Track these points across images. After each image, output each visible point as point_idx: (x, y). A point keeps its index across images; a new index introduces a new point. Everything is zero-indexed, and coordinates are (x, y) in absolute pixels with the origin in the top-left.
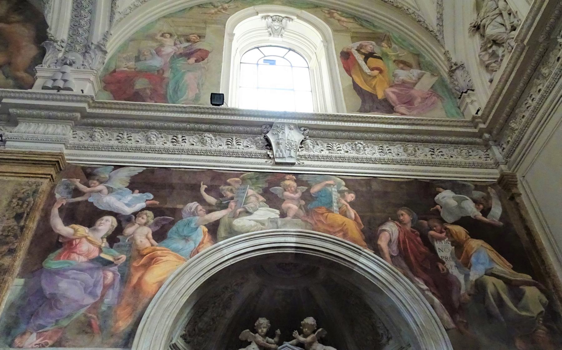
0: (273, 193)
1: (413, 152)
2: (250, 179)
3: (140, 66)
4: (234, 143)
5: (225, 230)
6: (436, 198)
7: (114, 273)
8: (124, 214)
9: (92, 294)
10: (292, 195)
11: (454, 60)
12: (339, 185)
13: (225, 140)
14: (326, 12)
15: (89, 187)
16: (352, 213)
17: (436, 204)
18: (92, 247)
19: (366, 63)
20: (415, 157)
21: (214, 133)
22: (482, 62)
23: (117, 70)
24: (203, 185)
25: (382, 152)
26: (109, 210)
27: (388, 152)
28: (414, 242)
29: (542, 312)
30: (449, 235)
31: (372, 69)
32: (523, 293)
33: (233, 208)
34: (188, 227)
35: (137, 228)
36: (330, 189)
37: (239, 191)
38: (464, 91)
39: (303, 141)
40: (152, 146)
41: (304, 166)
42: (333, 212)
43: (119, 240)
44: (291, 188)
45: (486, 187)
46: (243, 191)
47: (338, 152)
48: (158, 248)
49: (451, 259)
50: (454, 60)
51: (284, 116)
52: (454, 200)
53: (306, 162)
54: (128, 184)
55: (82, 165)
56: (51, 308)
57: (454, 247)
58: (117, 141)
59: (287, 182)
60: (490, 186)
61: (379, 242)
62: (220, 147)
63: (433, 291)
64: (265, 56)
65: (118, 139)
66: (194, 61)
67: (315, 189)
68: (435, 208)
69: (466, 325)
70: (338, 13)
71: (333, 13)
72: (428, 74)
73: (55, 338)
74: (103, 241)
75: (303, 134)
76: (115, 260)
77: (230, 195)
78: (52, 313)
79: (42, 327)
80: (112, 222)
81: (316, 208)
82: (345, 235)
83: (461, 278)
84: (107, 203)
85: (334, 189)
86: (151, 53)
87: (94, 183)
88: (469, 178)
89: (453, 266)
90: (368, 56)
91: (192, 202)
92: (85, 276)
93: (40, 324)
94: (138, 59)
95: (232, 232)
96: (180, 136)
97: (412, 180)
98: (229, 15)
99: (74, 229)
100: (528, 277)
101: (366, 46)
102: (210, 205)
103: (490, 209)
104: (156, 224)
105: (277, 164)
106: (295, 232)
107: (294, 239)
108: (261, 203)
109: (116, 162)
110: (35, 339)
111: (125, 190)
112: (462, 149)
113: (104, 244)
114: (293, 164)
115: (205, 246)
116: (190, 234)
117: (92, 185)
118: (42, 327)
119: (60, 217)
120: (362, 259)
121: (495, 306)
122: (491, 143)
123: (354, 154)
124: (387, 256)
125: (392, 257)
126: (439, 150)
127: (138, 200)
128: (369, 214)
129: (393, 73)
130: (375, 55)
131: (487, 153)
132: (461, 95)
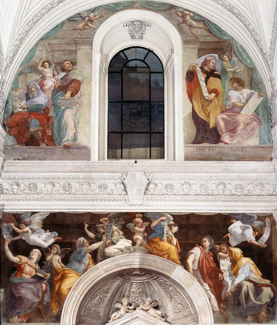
2: (114, 218)
5: (101, 256)
6: (229, 228)
7: (45, 284)
9: (37, 296)
10: (139, 229)
12: (169, 220)
14: (180, 14)
15: (20, 229)
16: (175, 241)
17: (228, 232)
23: (14, 111)
30: (230, 255)
31: (210, 92)
32: (261, 291)
33: (105, 240)
34: (80, 254)
35: (52, 257)
37: (107, 228)
41: (147, 206)
42: (163, 241)
43: (44, 265)
44: (139, 224)
46: (110, 228)
48: (66, 269)
52: (241, 229)
54: (42, 226)
55: (13, 213)
56: (21, 304)
57: (231, 263)
59: (137, 220)
61: (188, 261)
67: (154, 223)
68: (227, 236)
69: (225, 310)
70: (190, 16)
73: (26, 319)
74: (36, 265)
77: (102, 230)
78: (21, 307)
79: (19, 313)
80: (38, 253)
81: (153, 238)
82: (169, 258)
84: (33, 240)
86: (37, 89)
87: (23, 226)
89: (227, 275)
92: (32, 286)
93: (18, 312)
95: (105, 257)
98: (95, 30)
102: (91, 239)
103: (262, 235)
104: (62, 253)
108: (121, 236)
110: (18, 319)
111: (41, 230)
115: (90, 267)
116: (81, 259)
117: (22, 227)
118: (19, 313)
121: (244, 298)
124: (191, 270)
125: (194, 270)
128: (185, 242)
130: (216, 72)
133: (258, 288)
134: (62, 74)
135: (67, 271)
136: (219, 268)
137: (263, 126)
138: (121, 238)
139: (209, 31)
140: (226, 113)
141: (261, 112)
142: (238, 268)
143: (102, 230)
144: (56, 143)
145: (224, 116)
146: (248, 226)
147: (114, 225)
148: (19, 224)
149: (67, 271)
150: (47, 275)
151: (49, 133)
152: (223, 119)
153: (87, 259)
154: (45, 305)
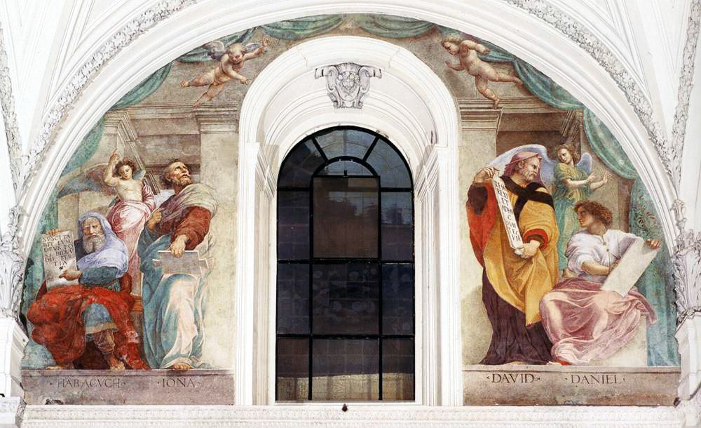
14: (454, 47)
23: (48, 285)
31: (527, 238)
70: (478, 51)
86: (102, 230)
98: (245, 85)
130: (540, 190)
134: (165, 194)
137: (655, 321)
139: (524, 88)
140: (567, 290)
141: (650, 288)
144: (150, 363)
145: (561, 296)
151: (133, 338)
152: (559, 304)
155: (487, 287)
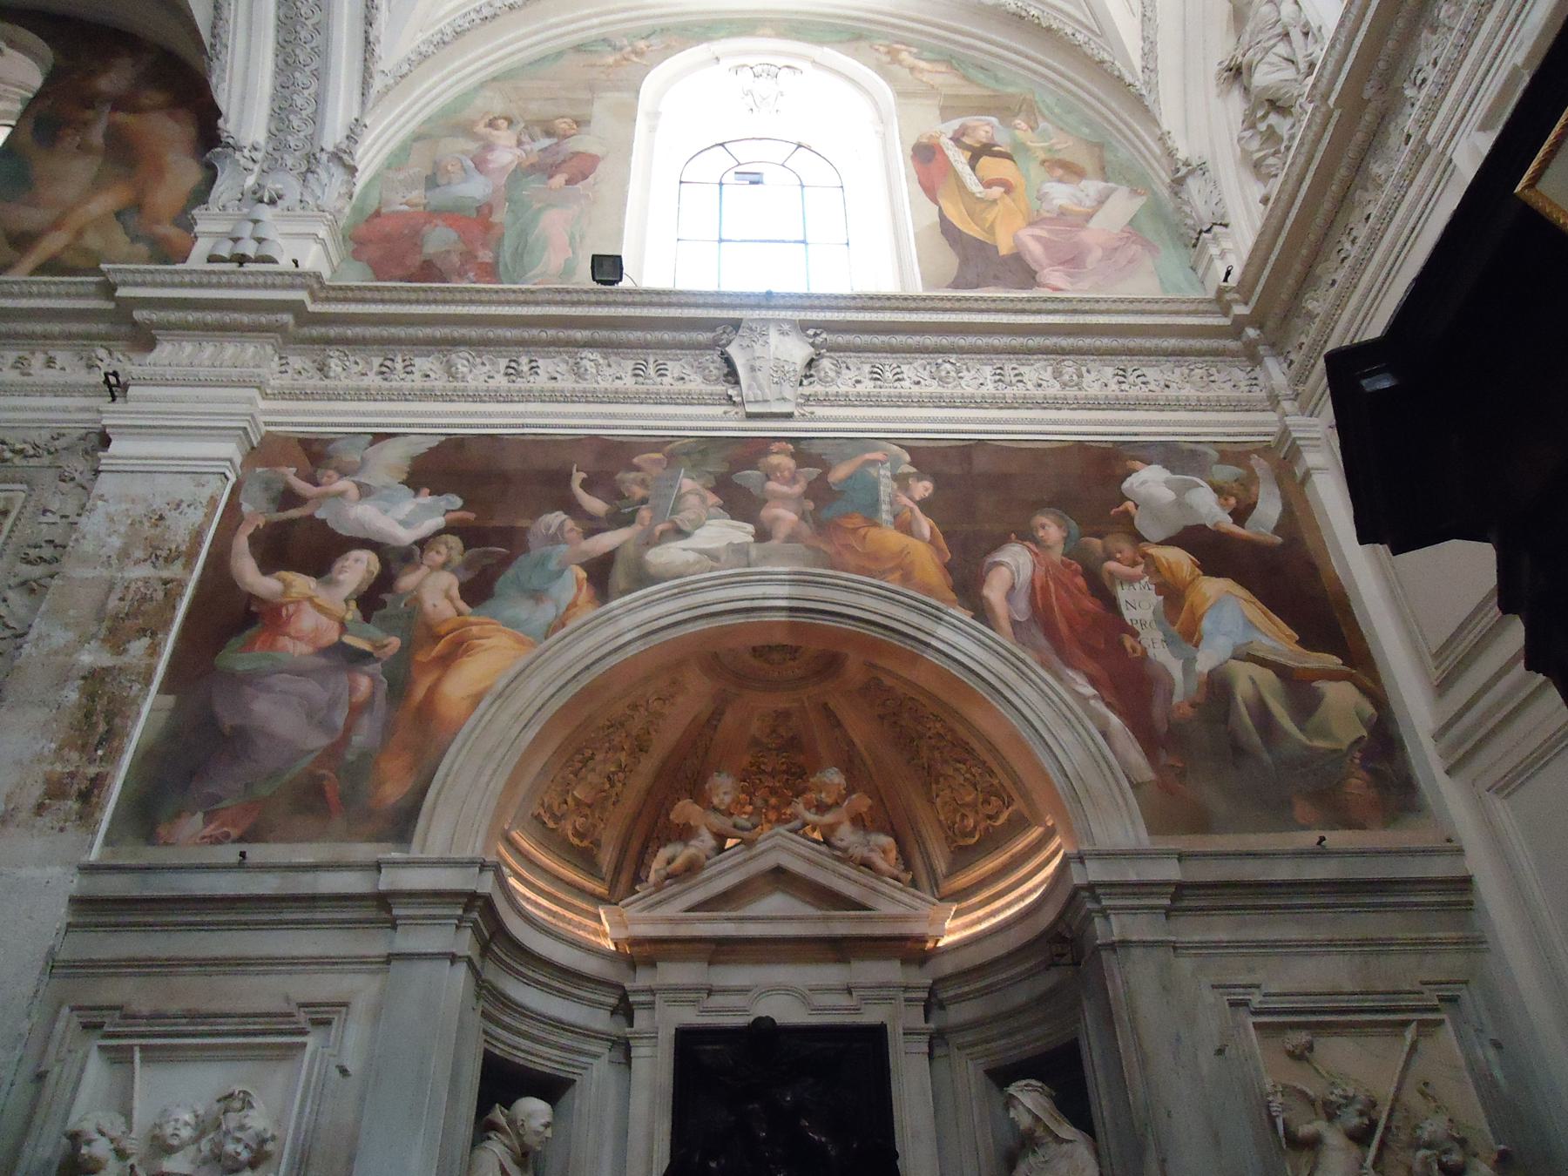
0: (740, 486)
1: (1075, 377)
2: (687, 454)
3: (438, 198)
4: (651, 371)
6: (1126, 485)
7: (372, 677)
8: (395, 544)
9: (324, 725)
10: (785, 489)
11: (1181, 155)
12: (896, 461)
13: (630, 365)
14: (882, 49)
15: (317, 484)
16: (925, 525)
17: (1124, 498)
18: (324, 619)
19: (973, 168)
20: (1080, 389)
21: (605, 350)
22: (1246, 154)
23: (384, 210)
24: (577, 471)
25: (1000, 380)
26: (361, 535)
27: (1014, 380)
28: (1067, 590)
29: (1362, 738)
30: (1153, 569)
31: (988, 185)
33: (647, 523)
36: (873, 471)
38: (1205, 229)
39: (812, 360)
40: (461, 385)
42: (876, 525)
43: (384, 604)
44: (781, 472)
45: (1247, 454)
47: (896, 384)
49: (1154, 624)
50: (1181, 155)
51: (767, 300)
53: (820, 411)
54: (404, 477)
55: (301, 436)
57: (1161, 598)
58: (380, 376)
59: (775, 460)
60: (1256, 451)
61: (986, 592)
62: (617, 381)
63: (1107, 700)
64: (739, 164)
65: (383, 373)
66: (564, 182)
67: (839, 473)
68: (1121, 508)
71: (899, 51)
72: (1122, 192)
75: (813, 345)
76: (376, 648)
77: (639, 492)
82: (906, 578)
83: (1176, 668)
85: (885, 472)
86: (464, 169)
87: (329, 477)
88: (1206, 434)
90: (977, 154)
91: (552, 512)
92: (311, 687)
94: (431, 182)
95: (643, 577)
96: (524, 360)
97: (1067, 444)
98: (647, 70)
99: (283, 581)
100: (1333, 661)
101: (975, 128)
102: (591, 517)
103: (1253, 506)
104: (468, 565)
105: (750, 416)
106: (789, 574)
107: (785, 590)
108: (711, 510)
109: (378, 425)
112: (1191, 367)
113: (350, 613)
114: (789, 416)
117: (325, 480)
119: (254, 555)
120: (942, 631)
122: (1262, 349)
123: (933, 388)
124: (1005, 625)
125: (1015, 624)
126: (1138, 373)
127: (428, 511)
129: (1038, 191)
130: (996, 149)
131: (1253, 375)
132: (1198, 239)
133: (1299, 689)
135: (475, 629)
136: (1120, 614)
138: (708, 519)
142: (1192, 611)
143: (639, 492)
146: (1192, 481)
147: (685, 477)
148: (315, 471)
149: (475, 629)
150: (385, 642)
153: (571, 584)
154: (352, 763)
155: (943, 218)
